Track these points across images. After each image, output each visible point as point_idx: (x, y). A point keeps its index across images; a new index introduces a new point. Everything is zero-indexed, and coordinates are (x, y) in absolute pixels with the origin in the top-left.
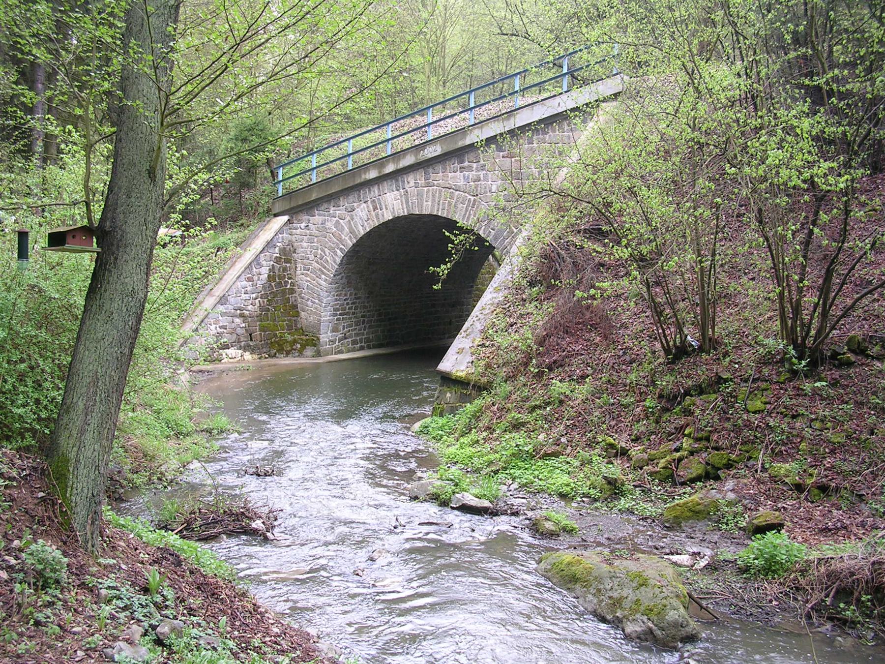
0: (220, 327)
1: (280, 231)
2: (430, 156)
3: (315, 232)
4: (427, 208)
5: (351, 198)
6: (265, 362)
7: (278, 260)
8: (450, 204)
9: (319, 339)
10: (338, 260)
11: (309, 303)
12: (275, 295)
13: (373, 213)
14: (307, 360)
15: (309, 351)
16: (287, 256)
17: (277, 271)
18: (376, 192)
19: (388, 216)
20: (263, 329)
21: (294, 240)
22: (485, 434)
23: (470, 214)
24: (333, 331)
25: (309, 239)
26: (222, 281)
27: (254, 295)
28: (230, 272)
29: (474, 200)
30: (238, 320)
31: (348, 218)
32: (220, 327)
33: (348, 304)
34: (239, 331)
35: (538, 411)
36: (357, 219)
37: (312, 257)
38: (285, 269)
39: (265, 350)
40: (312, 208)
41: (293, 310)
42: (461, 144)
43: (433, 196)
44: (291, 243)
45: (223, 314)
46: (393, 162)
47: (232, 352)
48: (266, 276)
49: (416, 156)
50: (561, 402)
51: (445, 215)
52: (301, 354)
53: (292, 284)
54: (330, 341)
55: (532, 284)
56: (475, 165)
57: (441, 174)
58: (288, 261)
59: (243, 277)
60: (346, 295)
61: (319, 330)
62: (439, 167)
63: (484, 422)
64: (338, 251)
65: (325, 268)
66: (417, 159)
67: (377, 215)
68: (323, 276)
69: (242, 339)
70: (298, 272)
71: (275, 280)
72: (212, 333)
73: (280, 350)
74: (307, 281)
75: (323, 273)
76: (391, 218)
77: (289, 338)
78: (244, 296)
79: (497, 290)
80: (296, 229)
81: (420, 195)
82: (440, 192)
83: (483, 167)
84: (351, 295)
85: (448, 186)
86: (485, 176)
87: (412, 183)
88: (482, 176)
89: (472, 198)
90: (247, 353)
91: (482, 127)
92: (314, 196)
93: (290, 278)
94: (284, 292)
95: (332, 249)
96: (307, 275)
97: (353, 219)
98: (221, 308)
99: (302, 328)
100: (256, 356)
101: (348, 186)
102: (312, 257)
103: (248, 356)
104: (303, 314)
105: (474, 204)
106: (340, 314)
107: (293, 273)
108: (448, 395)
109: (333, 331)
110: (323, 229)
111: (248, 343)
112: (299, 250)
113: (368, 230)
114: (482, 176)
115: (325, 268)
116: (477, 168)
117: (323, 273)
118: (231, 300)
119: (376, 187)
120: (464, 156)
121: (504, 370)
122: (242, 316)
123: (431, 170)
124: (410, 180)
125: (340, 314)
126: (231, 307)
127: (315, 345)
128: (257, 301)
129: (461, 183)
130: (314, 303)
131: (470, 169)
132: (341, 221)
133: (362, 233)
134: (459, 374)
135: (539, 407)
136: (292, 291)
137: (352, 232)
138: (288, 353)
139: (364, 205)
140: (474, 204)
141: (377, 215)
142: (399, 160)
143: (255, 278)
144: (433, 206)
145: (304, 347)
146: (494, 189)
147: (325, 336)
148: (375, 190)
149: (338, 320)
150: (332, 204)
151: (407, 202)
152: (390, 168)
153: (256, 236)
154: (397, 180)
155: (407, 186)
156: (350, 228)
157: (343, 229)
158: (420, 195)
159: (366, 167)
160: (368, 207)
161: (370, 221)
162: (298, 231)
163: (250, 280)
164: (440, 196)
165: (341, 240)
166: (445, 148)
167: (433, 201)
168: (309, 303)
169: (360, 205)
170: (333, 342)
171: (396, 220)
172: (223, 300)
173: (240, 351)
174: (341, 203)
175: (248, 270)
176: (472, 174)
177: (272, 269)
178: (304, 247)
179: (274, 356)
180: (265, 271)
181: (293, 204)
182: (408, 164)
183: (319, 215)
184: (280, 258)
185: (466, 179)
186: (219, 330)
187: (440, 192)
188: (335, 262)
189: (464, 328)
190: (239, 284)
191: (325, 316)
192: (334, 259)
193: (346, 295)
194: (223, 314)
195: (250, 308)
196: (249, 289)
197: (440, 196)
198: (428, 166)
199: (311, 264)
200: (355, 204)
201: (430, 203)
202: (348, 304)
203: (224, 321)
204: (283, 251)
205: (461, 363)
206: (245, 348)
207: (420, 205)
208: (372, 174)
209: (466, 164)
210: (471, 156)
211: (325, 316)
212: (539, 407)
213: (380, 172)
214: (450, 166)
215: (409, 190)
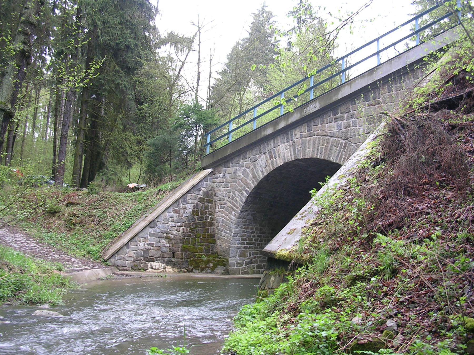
0: (148, 245)
1: (205, 178)
2: (311, 111)
3: (229, 179)
4: (309, 153)
5: (254, 152)
6: (181, 274)
7: (201, 200)
8: (326, 148)
9: (228, 261)
10: (244, 199)
11: (223, 233)
12: (197, 225)
13: (270, 161)
14: (218, 275)
15: (220, 269)
16: (209, 198)
17: (200, 208)
18: (272, 145)
19: (280, 162)
20: (184, 250)
21: (215, 186)
22: (287, 317)
23: (342, 155)
24: (240, 256)
25: (225, 185)
26: (155, 211)
27: (179, 224)
28: (162, 205)
29: (346, 143)
30: (163, 241)
31: (252, 167)
32: (148, 245)
33: (254, 236)
34: (164, 249)
35: (359, 284)
36: (258, 167)
37: (226, 198)
38: (206, 207)
39: (184, 266)
40: (228, 161)
41: (211, 238)
42: (334, 99)
43: (314, 143)
44: (212, 189)
45: (151, 235)
46: (285, 120)
47: (156, 264)
48: (191, 210)
49: (301, 113)
50: (395, 272)
51: (322, 158)
52: (213, 271)
53: (212, 219)
54: (238, 263)
55: (377, 163)
56: (346, 115)
57: (320, 125)
58: (210, 202)
59: (171, 209)
60: (252, 229)
61: (229, 254)
62: (319, 121)
63: (291, 301)
64: (244, 193)
65: (235, 206)
66: (301, 115)
67: (272, 163)
68: (233, 212)
69: (166, 255)
70: (217, 210)
71: (197, 215)
72: (140, 248)
73: (197, 267)
74: (223, 217)
75: (234, 210)
76: (282, 164)
77: (205, 258)
78: (170, 223)
79: (340, 178)
80: (217, 178)
81: (304, 143)
82: (319, 139)
83: (352, 116)
84: (256, 229)
85: (325, 134)
86: (354, 123)
87: (298, 136)
88: (351, 123)
89: (344, 142)
90: (169, 267)
91: (351, 84)
92: (229, 152)
93: (210, 215)
94: (204, 224)
95: (240, 191)
96: (222, 212)
97: (255, 167)
98: (151, 230)
99: (217, 253)
100: (176, 270)
101: (255, 142)
102: (226, 198)
103: (169, 269)
104: (218, 242)
105: (345, 146)
106: (247, 244)
107: (213, 211)
108: (272, 279)
109: (240, 256)
110: (235, 176)
111: (170, 259)
112: (218, 194)
113: (266, 174)
114: (351, 123)
115: (235, 206)
116: (347, 117)
117: (234, 210)
118: (160, 225)
119: (272, 141)
120: (337, 109)
121: (330, 242)
122: (167, 238)
123: (312, 124)
124: (297, 133)
125: (247, 244)
126: (158, 230)
127: (224, 265)
128: (181, 228)
129: (336, 130)
130: (226, 233)
131: (342, 118)
132: (247, 169)
133: (262, 177)
134: (282, 253)
135: (362, 278)
136: (211, 224)
137: (254, 177)
138: (202, 270)
139: (264, 156)
140: (345, 146)
141: (272, 163)
142: (288, 118)
143: (182, 211)
144: (313, 151)
145: (215, 266)
146: (361, 131)
147: (234, 259)
148: (272, 144)
149: (245, 247)
150: (242, 157)
151: (294, 150)
152: (282, 125)
153: (188, 182)
154: (287, 134)
155: (294, 138)
156: (253, 174)
157: (247, 176)
158: (304, 143)
159: (264, 127)
160: (266, 157)
161: (267, 168)
162: (218, 180)
163: (176, 212)
164: (319, 143)
165: (246, 184)
166: (322, 103)
167: (314, 147)
168: (223, 233)
169: (260, 156)
170: (241, 264)
171: (287, 165)
172: (151, 224)
173: (163, 265)
174: (248, 156)
175: (175, 205)
176: (343, 123)
177: (196, 206)
178: (222, 192)
179: (191, 271)
180: (190, 207)
181: (215, 159)
182: (295, 120)
183: (233, 167)
184: (204, 199)
185: (339, 127)
186: (147, 246)
187: (319, 139)
188: (242, 201)
189: (301, 211)
190: (167, 214)
191: (234, 243)
192: (241, 199)
193: (252, 229)
194: (151, 235)
195: (174, 232)
196: (175, 218)
197: (319, 143)
198: (310, 121)
199: (225, 204)
200: (257, 156)
201: (311, 149)
202: (254, 236)
203: (152, 240)
204: (206, 194)
205: (289, 243)
206: (168, 263)
207: (304, 152)
208: (269, 131)
209: (339, 115)
210: (343, 108)
211: (234, 243)
212: (362, 278)
213: (274, 129)
214: (326, 118)
215: (296, 140)
